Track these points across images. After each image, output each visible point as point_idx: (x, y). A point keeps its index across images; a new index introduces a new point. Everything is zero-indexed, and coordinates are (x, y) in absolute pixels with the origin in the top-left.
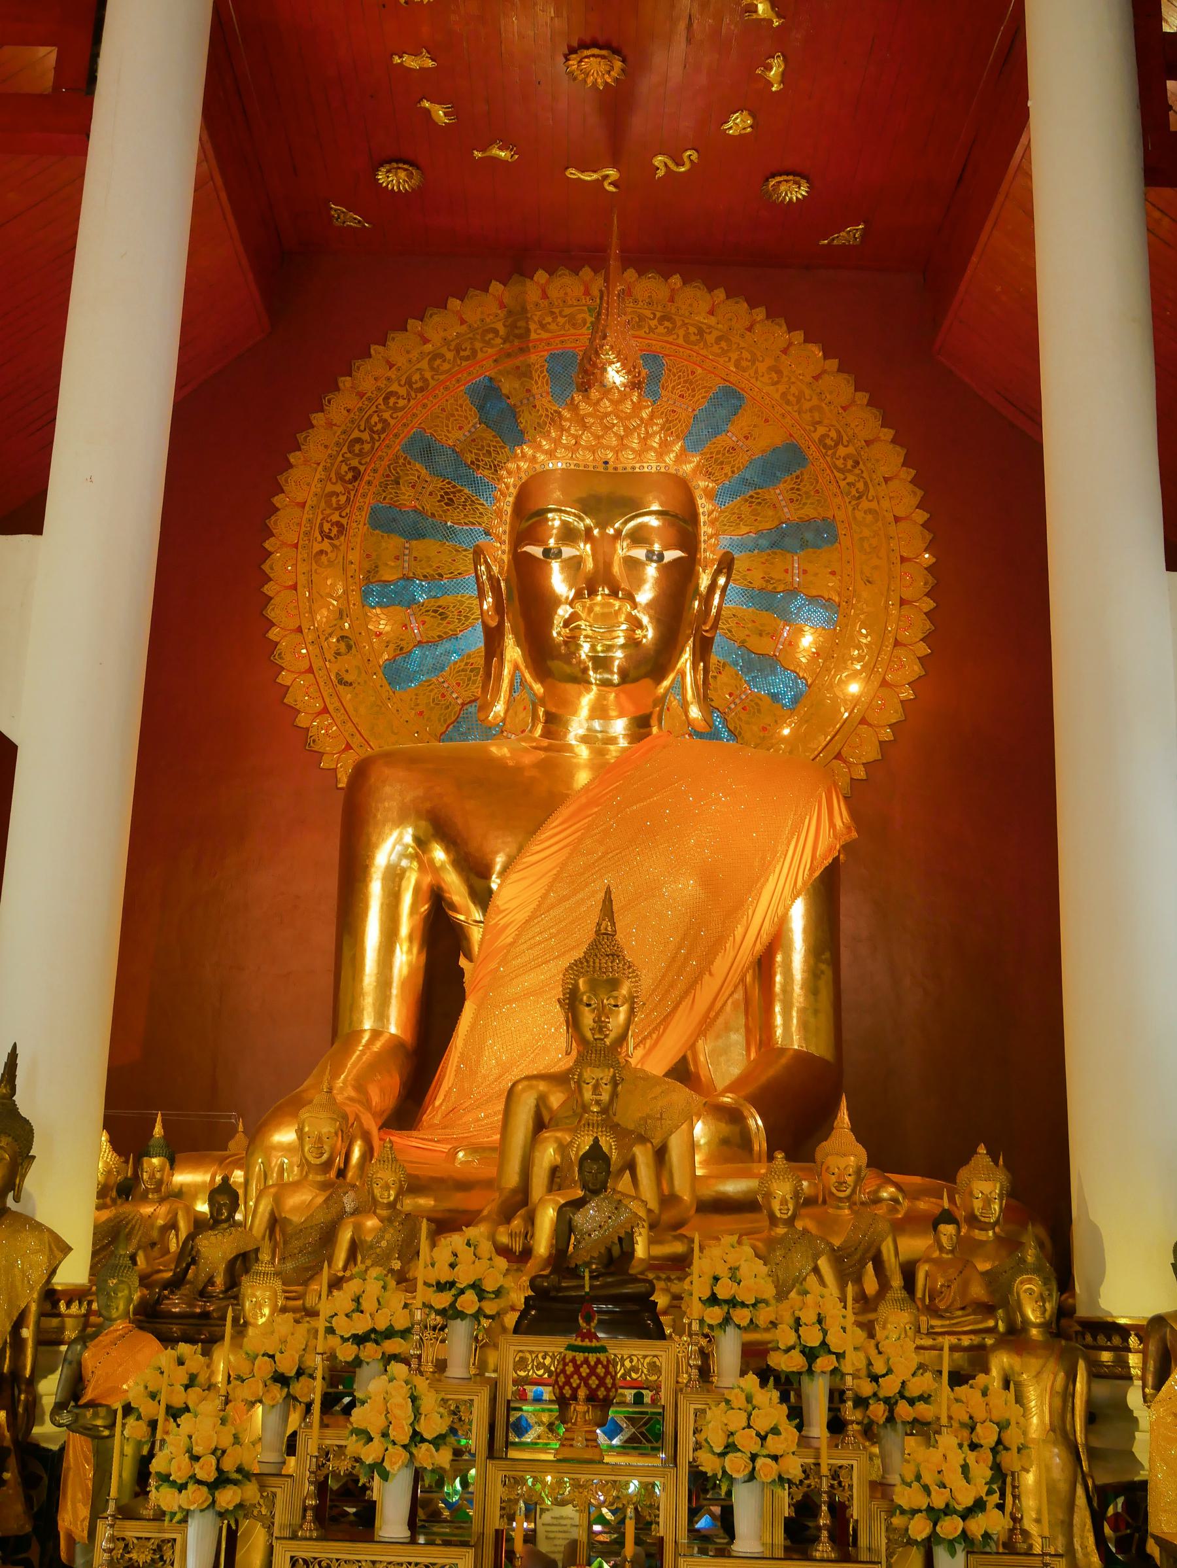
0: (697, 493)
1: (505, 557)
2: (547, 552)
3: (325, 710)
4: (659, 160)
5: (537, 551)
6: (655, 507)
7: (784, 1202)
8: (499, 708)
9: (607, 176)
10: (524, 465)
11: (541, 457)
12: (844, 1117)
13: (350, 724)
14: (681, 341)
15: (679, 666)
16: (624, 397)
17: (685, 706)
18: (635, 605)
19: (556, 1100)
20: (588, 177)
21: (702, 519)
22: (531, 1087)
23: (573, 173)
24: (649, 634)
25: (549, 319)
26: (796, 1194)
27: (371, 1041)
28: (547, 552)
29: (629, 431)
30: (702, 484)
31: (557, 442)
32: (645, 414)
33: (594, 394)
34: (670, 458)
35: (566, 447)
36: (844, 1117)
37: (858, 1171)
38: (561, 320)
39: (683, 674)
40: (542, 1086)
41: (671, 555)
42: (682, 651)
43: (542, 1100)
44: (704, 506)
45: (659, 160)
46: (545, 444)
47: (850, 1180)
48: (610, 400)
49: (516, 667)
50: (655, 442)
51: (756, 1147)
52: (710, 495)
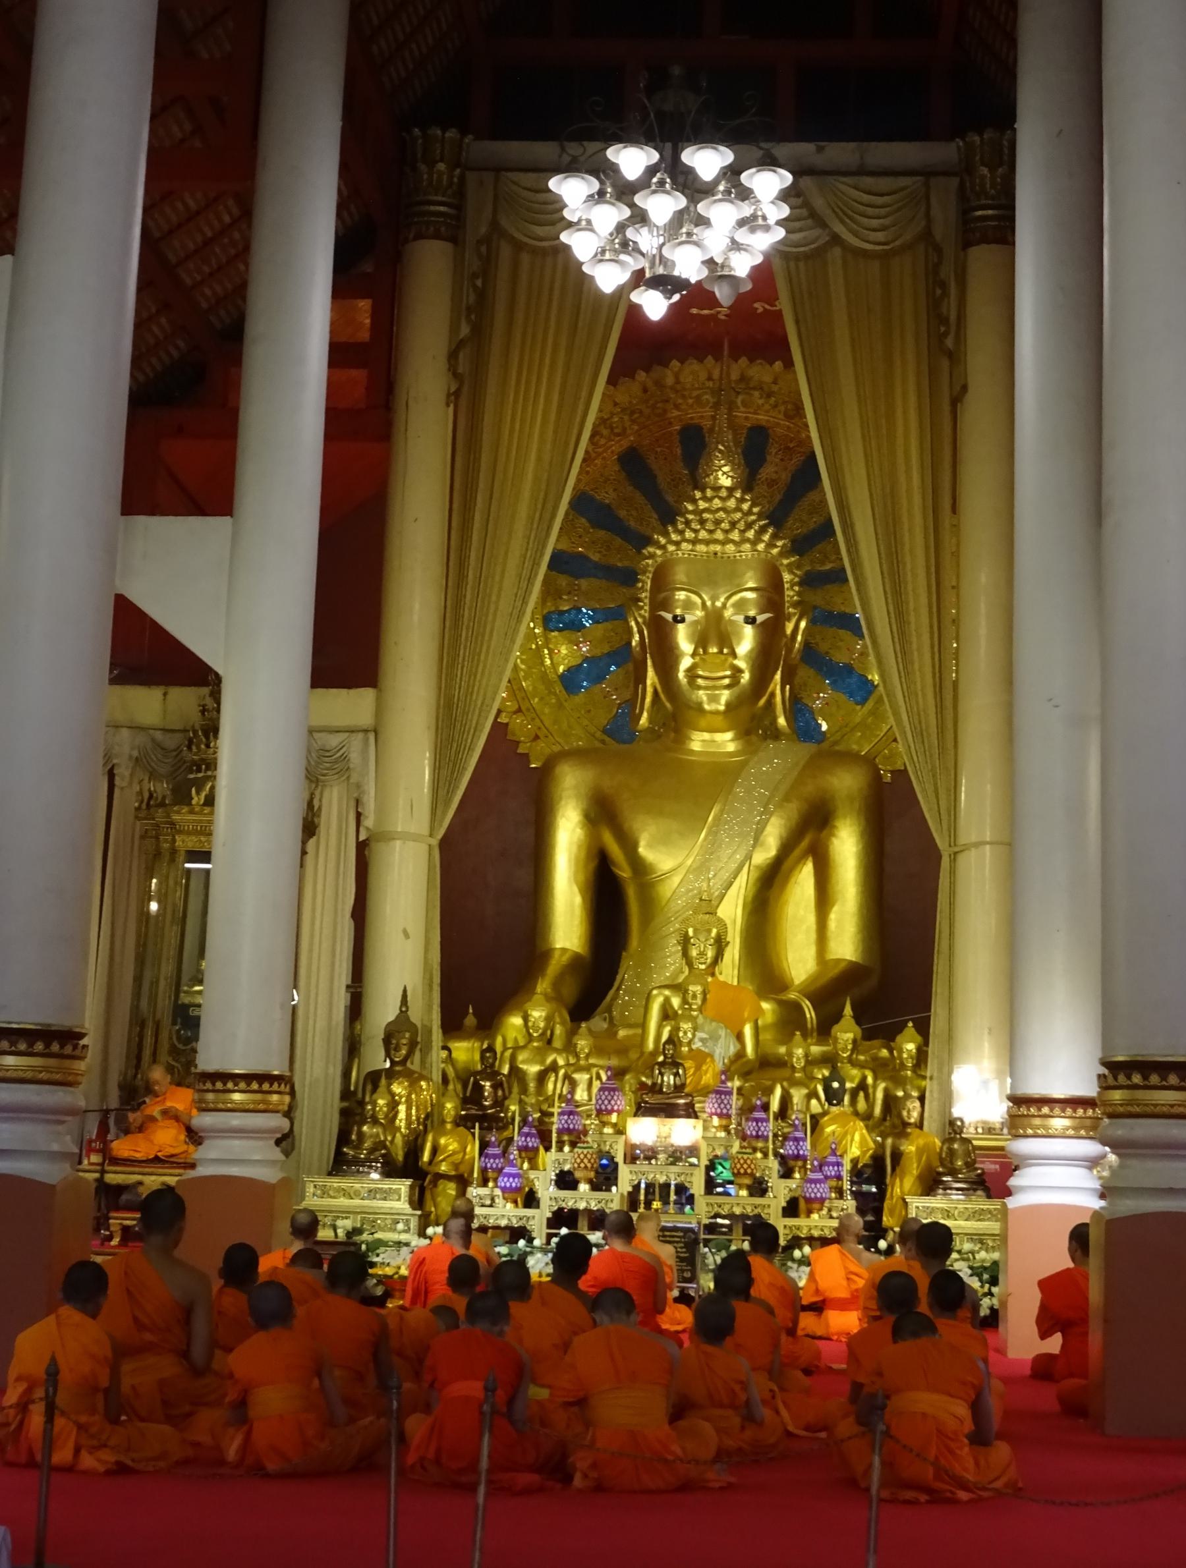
0: (781, 568)
1: (647, 615)
2: (675, 618)
3: (519, 710)
4: (756, 305)
5: (669, 617)
6: (751, 584)
7: (798, 1059)
8: (644, 720)
9: (719, 312)
10: (659, 552)
11: (671, 548)
12: (848, 1011)
13: (537, 720)
14: (781, 416)
15: (770, 690)
16: (730, 495)
17: (775, 719)
18: (735, 655)
19: (676, 1002)
20: (706, 312)
21: (786, 586)
22: (660, 994)
23: (694, 311)
24: (746, 677)
25: (680, 401)
26: (806, 1055)
27: (561, 955)
28: (675, 618)
29: (733, 524)
30: (785, 562)
31: (682, 532)
32: (745, 506)
33: (709, 493)
34: (761, 547)
35: (688, 541)
36: (848, 1011)
37: (855, 1041)
38: (690, 401)
39: (773, 695)
40: (667, 992)
41: (760, 618)
42: (774, 673)
43: (667, 1001)
44: (787, 577)
45: (756, 305)
46: (674, 537)
47: (850, 1047)
48: (720, 498)
49: (655, 692)
50: (751, 534)
51: (809, 1025)
52: (790, 568)
